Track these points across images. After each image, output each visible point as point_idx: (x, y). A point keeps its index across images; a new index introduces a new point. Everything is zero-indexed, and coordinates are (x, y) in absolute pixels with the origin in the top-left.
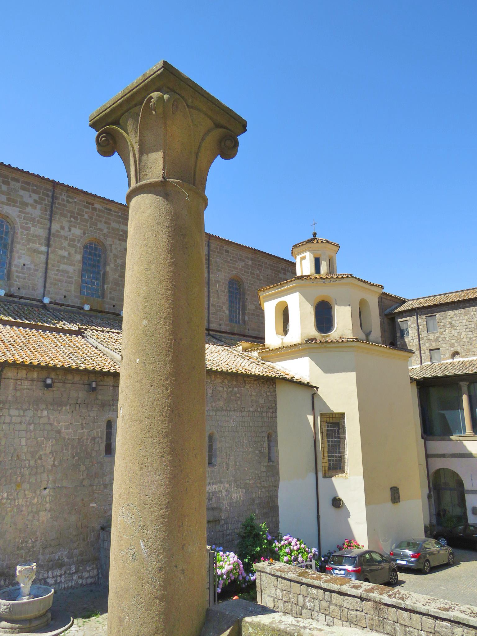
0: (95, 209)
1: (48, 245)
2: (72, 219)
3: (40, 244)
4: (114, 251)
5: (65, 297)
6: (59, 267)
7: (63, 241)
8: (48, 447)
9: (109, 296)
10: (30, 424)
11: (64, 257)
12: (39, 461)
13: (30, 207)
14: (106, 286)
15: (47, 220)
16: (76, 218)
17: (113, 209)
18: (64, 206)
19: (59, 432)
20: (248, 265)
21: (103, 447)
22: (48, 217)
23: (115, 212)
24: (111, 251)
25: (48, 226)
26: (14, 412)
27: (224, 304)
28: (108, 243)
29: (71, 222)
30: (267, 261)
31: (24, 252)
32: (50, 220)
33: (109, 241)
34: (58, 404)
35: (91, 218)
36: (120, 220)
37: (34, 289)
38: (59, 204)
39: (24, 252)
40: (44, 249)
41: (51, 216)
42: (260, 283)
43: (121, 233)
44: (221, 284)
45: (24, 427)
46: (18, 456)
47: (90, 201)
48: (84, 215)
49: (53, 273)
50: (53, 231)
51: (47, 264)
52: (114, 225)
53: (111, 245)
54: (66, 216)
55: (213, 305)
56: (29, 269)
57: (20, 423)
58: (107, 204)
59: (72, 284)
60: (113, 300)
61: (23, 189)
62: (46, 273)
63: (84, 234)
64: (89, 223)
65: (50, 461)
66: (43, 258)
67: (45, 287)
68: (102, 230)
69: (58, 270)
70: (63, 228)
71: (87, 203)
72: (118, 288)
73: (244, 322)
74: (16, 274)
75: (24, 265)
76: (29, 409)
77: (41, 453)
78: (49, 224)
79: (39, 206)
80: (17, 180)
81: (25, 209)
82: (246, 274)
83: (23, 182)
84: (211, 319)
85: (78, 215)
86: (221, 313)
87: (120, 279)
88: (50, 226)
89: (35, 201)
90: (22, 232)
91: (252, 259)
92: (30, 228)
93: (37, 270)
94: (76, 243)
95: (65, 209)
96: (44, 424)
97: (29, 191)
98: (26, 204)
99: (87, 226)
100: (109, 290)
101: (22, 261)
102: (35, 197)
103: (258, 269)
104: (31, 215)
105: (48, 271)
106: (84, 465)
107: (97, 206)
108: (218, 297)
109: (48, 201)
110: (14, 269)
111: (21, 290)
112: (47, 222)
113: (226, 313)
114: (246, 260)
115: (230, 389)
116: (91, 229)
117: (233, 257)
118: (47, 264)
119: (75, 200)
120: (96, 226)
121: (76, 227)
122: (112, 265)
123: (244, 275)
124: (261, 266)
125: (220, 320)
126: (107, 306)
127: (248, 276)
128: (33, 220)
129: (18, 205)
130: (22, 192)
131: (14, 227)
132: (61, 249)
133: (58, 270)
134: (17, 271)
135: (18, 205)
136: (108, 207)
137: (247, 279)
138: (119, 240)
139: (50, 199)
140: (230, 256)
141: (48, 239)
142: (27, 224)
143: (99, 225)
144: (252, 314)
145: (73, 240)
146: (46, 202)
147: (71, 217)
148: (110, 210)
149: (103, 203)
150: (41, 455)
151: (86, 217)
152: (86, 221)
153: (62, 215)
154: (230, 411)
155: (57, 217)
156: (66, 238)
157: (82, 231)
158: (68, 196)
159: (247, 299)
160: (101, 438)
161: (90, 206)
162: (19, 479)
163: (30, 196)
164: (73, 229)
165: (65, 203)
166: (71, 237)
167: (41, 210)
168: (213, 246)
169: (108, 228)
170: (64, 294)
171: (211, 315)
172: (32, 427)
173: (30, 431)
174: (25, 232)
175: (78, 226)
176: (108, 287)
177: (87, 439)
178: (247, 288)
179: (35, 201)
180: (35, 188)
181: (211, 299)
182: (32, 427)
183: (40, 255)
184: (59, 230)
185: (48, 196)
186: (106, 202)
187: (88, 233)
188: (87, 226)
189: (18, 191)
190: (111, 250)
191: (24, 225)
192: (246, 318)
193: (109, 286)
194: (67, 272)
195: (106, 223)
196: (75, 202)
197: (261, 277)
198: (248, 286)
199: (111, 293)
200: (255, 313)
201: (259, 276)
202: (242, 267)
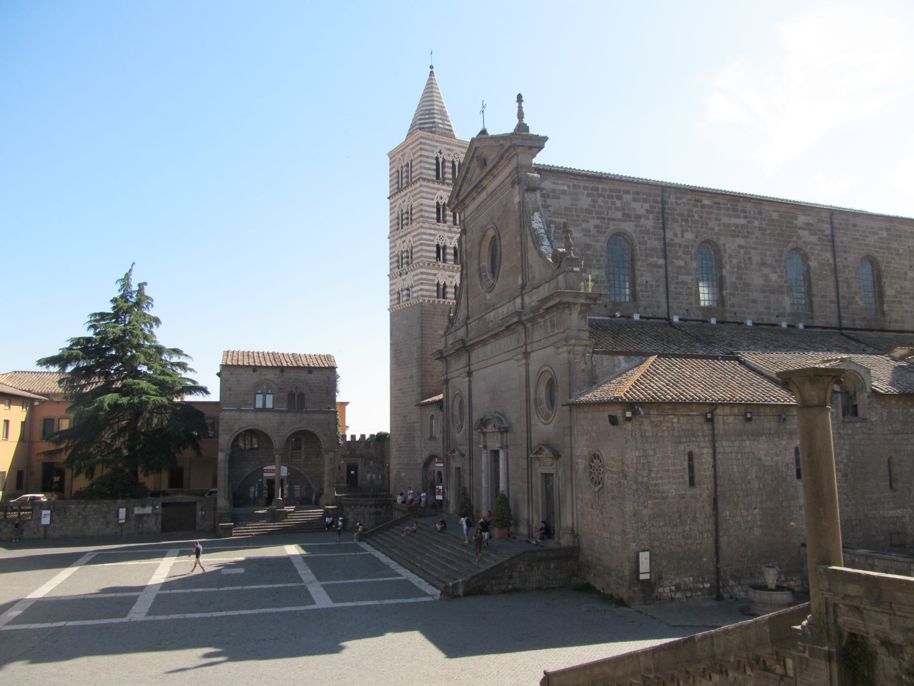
0: (703, 206)
1: (665, 257)
2: (684, 223)
3: (658, 257)
4: (729, 251)
5: (687, 310)
6: (678, 278)
7: (677, 249)
8: (754, 471)
9: (729, 303)
10: (737, 453)
11: (681, 267)
12: (748, 485)
13: (643, 219)
14: (724, 293)
15: (660, 229)
16: (686, 221)
17: (721, 201)
18: (675, 209)
19: (760, 459)
20: (882, 238)
21: (794, 472)
22: (661, 226)
23: (724, 204)
24: (726, 252)
25: (662, 236)
26: (725, 444)
27: (856, 293)
28: (721, 242)
29: (682, 226)
30: (907, 228)
31: (644, 269)
32: (664, 229)
33: (722, 240)
34: (756, 435)
35: (701, 217)
36: (730, 212)
37: (659, 307)
38: (669, 208)
39: (644, 269)
40: (661, 262)
41: (664, 224)
42: (900, 259)
43: (733, 228)
44: (851, 269)
45: (733, 456)
46: (733, 481)
47: (698, 198)
48: (693, 216)
49: (673, 286)
50: (668, 240)
51: (667, 278)
52: (725, 220)
53: (724, 245)
54: (677, 222)
55: (844, 297)
56: (651, 286)
57: (731, 453)
58: (715, 198)
59: (692, 295)
60: (734, 307)
61: (635, 200)
62: (667, 287)
63: (697, 237)
64: (700, 223)
65: (756, 484)
66: (662, 271)
67: (668, 303)
68: (713, 229)
69: (677, 283)
70: (675, 235)
71: (696, 201)
72: (737, 293)
73: (883, 313)
74: (641, 293)
75: (646, 282)
76: (736, 441)
77: (749, 478)
78: (662, 233)
79: (651, 216)
80: (627, 192)
81: (639, 222)
82: (881, 250)
83: (634, 193)
84: (843, 315)
85: (689, 217)
86: (853, 306)
87: (738, 282)
88: (665, 235)
89: (647, 211)
90: (640, 248)
91: (888, 230)
92: (646, 241)
93: (658, 286)
94: (690, 249)
95: (675, 212)
96: (748, 453)
97: (640, 202)
98: (639, 217)
99: (697, 228)
100: (728, 297)
101: (644, 279)
102: (647, 206)
103: (896, 241)
104: (646, 227)
105: (669, 285)
106: (782, 488)
107: (706, 202)
108: (849, 286)
109: (659, 208)
110: (638, 288)
111: (648, 309)
112: (661, 232)
113: (859, 305)
114: (880, 232)
115: (905, 411)
116: (702, 230)
117: (864, 231)
118: (667, 278)
119: (684, 200)
120: (707, 224)
121: (688, 232)
122: (728, 267)
123: (877, 252)
124: (900, 236)
125: (854, 314)
126: (728, 315)
127: (884, 253)
128: (647, 232)
129: (633, 219)
130: (634, 205)
131: (632, 244)
132: (678, 258)
133: (677, 283)
134: (642, 291)
135: (633, 219)
136: (716, 200)
137: (882, 257)
138: (733, 236)
139: (660, 205)
140: (858, 231)
141: (665, 250)
142: (643, 237)
143: (712, 224)
144: (893, 302)
145: (687, 246)
146: (657, 210)
147: (682, 220)
148: (719, 203)
149: (712, 197)
150: (749, 480)
151: (696, 217)
152: (697, 222)
153: (674, 221)
154: (907, 433)
155: (669, 223)
156: (680, 245)
157: (694, 234)
158: (677, 198)
159: (884, 283)
160: (792, 464)
161: (699, 204)
162: (736, 499)
163: (642, 207)
164: (685, 234)
165: (674, 206)
166: (685, 243)
167: (653, 219)
168: (836, 222)
169: (719, 225)
170: (686, 308)
171: (842, 310)
172: (739, 456)
173: (739, 459)
174: (643, 247)
175: (689, 229)
176: (726, 293)
177: (782, 465)
178: (883, 268)
179: (647, 211)
180: (645, 196)
181: (841, 290)
182: (739, 456)
183: (659, 269)
184: (673, 238)
185: (657, 202)
186: (714, 195)
187: (700, 236)
188: (697, 228)
189: (630, 204)
190: (725, 250)
191: (641, 239)
192: (886, 308)
193: (728, 291)
194: (686, 283)
195: (716, 219)
196: (684, 202)
197: (901, 251)
198: (885, 266)
199: (730, 299)
200: (896, 299)
201: (899, 251)
202: (875, 242)
